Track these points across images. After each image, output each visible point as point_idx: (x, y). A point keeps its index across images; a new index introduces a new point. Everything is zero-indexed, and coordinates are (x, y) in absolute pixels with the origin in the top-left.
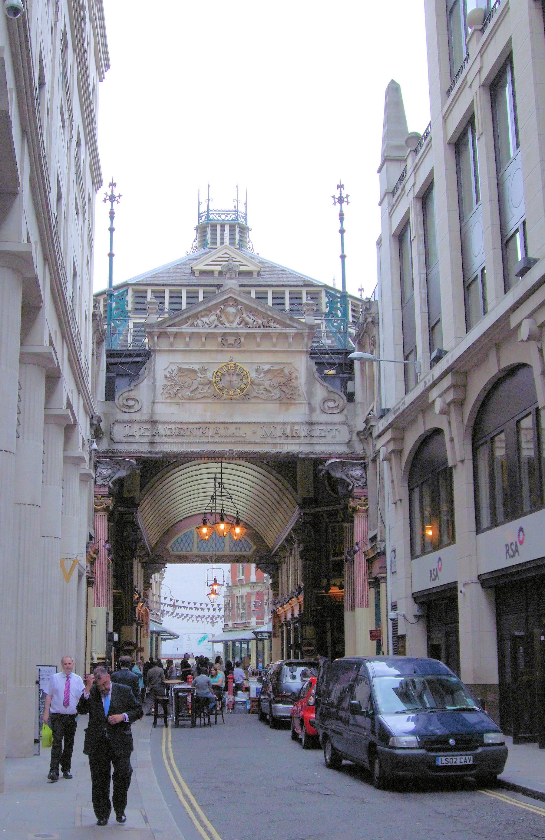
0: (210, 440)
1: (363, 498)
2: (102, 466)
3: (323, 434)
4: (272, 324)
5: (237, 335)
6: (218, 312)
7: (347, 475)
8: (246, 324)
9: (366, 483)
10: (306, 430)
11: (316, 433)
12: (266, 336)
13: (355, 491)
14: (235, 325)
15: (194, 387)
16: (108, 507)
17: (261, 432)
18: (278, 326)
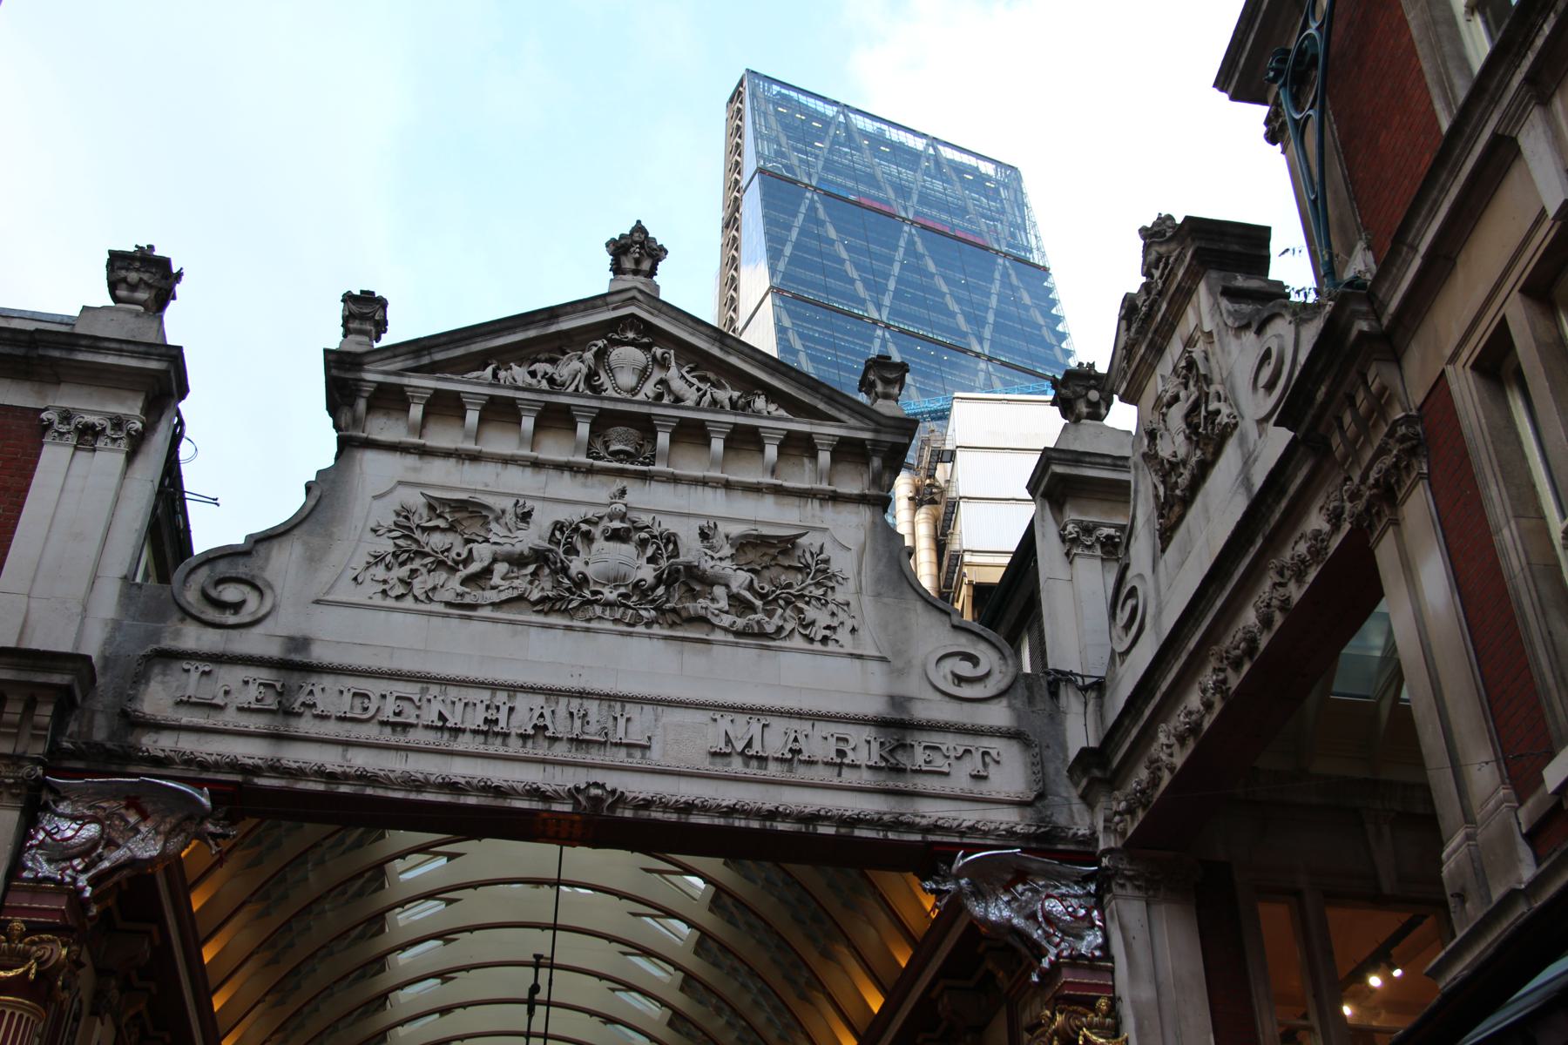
0: (514, 747)
1: (1103, 1004)
2: (64, 807)
3: (940, 763)
4: (760, 403)
5: (645, 426)
6: (589, 355)
7: (1032, 916)
8: (678, 400)
9: (1105, 947)
10: (875, 746)
11: (920, 757)
12: (745, 440)
13: (1067, 976)
14: (640, 397)
15: (474, 567)
16: (46, 974)
17: (711, 733)
18: (782, 412)
